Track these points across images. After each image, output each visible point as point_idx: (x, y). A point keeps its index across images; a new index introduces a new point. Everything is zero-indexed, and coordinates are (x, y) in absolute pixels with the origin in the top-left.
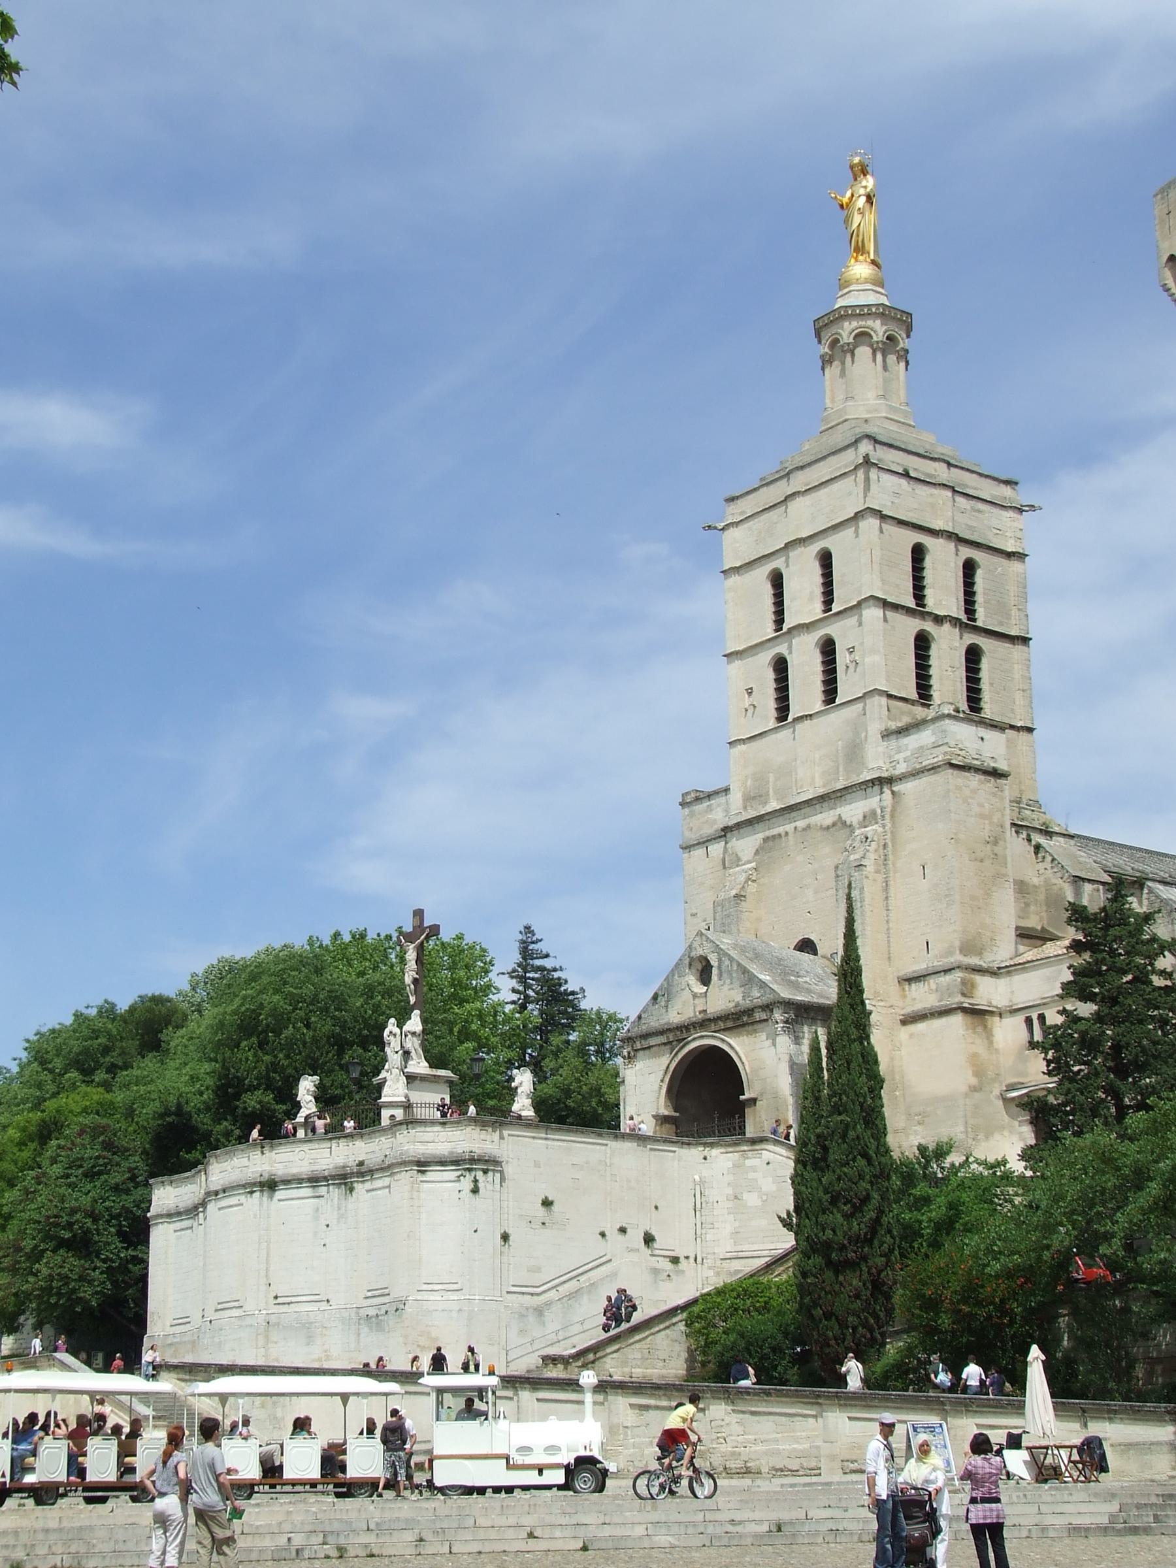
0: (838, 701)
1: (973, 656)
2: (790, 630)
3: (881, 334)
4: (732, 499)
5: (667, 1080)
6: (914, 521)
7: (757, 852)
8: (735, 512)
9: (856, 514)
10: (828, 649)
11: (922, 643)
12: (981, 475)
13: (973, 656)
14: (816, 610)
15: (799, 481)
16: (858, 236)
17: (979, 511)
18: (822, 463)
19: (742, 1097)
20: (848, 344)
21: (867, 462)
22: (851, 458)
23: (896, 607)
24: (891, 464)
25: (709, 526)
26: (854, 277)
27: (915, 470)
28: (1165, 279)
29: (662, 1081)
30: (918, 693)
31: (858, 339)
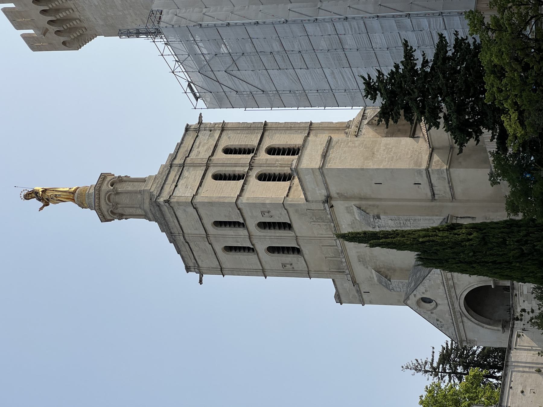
0: (289, 222)
1: (272, 151)
2: (253, 245)
5: (483, 324)
7: (367, 268)
9: (194, 208)
10: (263, 225)
11: (263, 177)
13: (272, 151)
14: (242, 232)
19: (493, 287)
20: (113, 206)
23: (242, 190)
27: (175, 176)
29: (483, 327)
30: (288, 181)
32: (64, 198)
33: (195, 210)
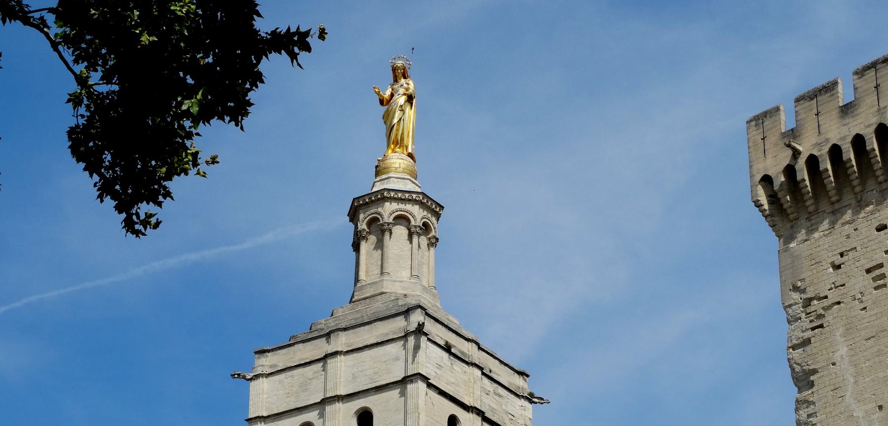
3: (419, 220)
4: (262, 352)
6: (451, 394)
8: (265, 363)
12: (501, 362)
15: (341, 342)
16: (397, 130)
17: (500, 396)
18: (367, 327)
21: (420, 330)
22: (398, 325)
24: (436, 337)
25: (239, 375)
26: (393, 165)
28: (757, 195)
31: (397, 221)
32: (397, 135)
33: (400, 379)
